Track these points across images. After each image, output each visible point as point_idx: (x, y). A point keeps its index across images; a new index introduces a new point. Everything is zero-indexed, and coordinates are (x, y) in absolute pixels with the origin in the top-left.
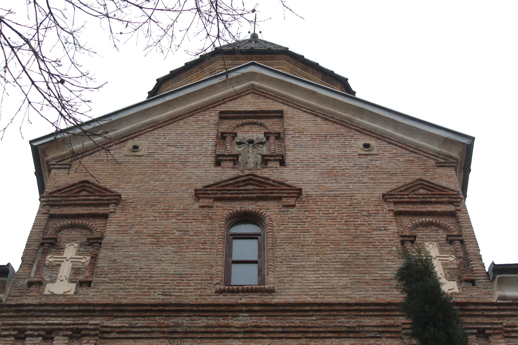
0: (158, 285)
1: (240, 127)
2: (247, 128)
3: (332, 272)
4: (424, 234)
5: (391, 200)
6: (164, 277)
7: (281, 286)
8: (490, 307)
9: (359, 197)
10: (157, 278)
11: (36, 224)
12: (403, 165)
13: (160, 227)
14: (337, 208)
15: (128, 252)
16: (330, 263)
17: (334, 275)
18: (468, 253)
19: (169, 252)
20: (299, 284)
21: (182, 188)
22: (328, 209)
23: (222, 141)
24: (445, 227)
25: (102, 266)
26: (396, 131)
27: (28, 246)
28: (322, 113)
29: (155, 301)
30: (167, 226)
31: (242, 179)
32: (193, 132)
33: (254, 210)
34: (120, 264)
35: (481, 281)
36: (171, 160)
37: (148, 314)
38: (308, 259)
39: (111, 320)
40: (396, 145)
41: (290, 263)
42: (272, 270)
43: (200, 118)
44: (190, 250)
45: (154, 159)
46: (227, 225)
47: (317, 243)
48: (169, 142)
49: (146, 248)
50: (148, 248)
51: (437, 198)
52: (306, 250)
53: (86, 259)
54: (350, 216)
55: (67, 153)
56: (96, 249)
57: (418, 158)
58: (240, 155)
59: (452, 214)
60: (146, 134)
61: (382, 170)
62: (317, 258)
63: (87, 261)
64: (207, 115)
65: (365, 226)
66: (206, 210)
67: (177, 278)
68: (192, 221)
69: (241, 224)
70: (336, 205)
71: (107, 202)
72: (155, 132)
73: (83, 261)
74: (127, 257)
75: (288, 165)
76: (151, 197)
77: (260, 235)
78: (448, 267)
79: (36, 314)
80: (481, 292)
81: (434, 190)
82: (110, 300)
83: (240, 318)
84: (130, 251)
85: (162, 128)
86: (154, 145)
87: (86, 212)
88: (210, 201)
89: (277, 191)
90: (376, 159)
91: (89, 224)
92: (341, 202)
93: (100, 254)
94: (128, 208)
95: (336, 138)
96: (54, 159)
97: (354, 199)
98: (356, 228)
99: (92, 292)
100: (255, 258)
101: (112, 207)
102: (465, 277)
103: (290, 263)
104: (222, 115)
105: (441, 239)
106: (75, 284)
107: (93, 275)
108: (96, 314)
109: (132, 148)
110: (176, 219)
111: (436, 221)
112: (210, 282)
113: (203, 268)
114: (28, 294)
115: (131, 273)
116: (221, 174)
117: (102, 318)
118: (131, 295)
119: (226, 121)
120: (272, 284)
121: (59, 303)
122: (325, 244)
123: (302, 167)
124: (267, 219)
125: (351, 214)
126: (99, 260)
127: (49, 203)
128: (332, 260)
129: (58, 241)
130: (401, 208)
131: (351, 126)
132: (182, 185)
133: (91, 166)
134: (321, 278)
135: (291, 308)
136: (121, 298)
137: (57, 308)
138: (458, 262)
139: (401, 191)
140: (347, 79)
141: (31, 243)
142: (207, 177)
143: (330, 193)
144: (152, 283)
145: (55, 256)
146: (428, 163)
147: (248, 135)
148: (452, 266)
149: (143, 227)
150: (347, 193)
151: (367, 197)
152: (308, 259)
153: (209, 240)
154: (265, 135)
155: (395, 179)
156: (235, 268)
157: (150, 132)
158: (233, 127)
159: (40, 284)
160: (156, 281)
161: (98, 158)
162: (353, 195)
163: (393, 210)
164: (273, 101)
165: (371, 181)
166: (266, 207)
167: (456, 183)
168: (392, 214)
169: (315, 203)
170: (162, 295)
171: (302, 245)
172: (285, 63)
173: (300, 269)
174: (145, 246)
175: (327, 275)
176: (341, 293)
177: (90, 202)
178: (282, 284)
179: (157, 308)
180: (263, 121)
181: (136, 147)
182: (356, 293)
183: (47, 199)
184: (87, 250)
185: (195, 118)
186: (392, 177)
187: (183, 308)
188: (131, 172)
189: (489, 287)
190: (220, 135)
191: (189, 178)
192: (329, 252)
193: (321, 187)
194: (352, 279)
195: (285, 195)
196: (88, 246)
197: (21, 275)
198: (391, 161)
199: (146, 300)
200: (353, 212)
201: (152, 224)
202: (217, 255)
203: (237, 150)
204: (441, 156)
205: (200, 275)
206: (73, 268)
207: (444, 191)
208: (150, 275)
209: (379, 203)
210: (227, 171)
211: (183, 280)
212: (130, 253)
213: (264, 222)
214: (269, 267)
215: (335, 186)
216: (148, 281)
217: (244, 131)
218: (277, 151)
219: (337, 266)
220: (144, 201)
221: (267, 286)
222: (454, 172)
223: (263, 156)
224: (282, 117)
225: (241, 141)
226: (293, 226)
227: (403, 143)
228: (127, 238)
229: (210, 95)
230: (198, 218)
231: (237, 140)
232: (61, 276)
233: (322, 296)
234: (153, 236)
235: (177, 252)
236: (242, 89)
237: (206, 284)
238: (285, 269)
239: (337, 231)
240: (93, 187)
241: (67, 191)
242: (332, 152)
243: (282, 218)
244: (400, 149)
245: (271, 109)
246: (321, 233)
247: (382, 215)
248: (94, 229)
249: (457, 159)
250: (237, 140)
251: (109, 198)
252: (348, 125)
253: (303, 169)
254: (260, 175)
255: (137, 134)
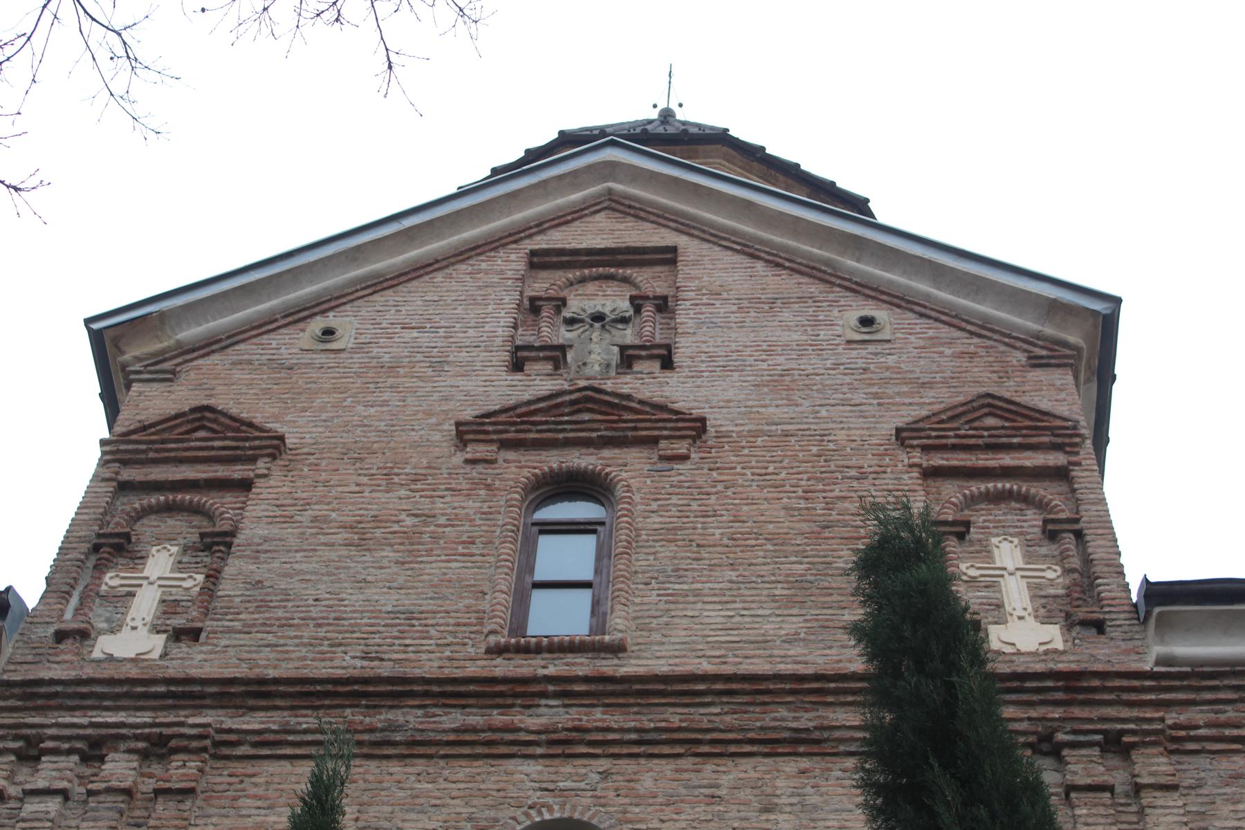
0: (355, 635)
1: (576, 286)
2: (591, 287)
3: (764, 605)
4: (991, 518)
5: (915, 442)
6: (369, 618)
7: (641, 636)
8: (1136, 683)
9: (841, 435)
10: (352, 621)
11: (86, 502)
12: (953, 364)
13: (370, 506)
14: (787, 461)
15: (291, 563)
16: (760, 586)
17: (768, 612)
18: (1092, 560)
19: (385, 563)
20: (684, 633)
21: (429, 421)
22: (766, 465)
23: (531, 317)
24: (1041, 501)
25: (229, 596)
26: (938, 289)
27: (65, 551)
28: (767, 250)
29: (344, 672)
30: (386, 506)
31: (567, 398)
32: (463, 298)
33: (591, 467)
34: (270, 590)
35: (1118, 623)
36: (408, 359)
37: (327, 702)
38: (711, 576)
39: (241, 716)
40: (936, 320)
41: (667, 585)
42: (623, 601)
43: (484, 266)
44: (434, 558)
45: (369, 357)
46: (527, 503)
47: (734, 539)
48: (407, 321)
49: (334, 555)
50: (339, 553)
51: (1024, 436)
52: (706, 555)
53: (195, 580)
54: (817, 478)
55: (169, 347)
56: (219, 557)
57: (986, 347)
58: (571, 346)
59: (1061, 474)
60: (356, 303)
61: (899, 376)
62: (731, 573)
63: (195, 586)
64: (500, 260)
65: (851, 502)
66: (480, 468)
67: (398, 621)
68: (446, 493)
69: (562, 501)
70: (784, 456)
71: (251, 452)
72: (376, 297)
73: (186, 584)
74: (286, 575)
75: (679, 367)
76: (356, 442)
77: (602, 524)
78: (1043, 593)
79: (69, 703)
80: (1118, 647)
81: (1019, 419)
82: (242, 671)
83: (543, 710)
84: (297, 562)
85: (394, 289)
86: (371, 327)
87: (204, 476)
88: (489, 448)
89: (648, 425)
90: (887, 351)
91: (206, 502)
92: (797, 448)
93: (226, 568)
94: (300, 466)
95: (797, 305)
96: (138, 359)
97: (829, 441)
98: (829, 506)
99: (201, 652)
100: (587, 574)
101: (261, 465)
102: (1081, 614)
103: (667, 585)
104: (535, 259)
105: (1030, 530)
106: (164, 636)
107: (206, 615)
108: (208, 702)
109: (320, 334)
110: (410, 490)
111: (1020, 488)
112: (475, 628)
113: (461, 598)
114: (52, 658)
115: (293, 609)
116: (523, 388)
117: (221, 712)
118: (291, 659)
119: (544, 274)
120: (621, 631)
121: (122, 676)
122: (753, 542)
123: (711, 371)
124: (619, 486)
125: (819, 475)
126: (223, 581)
127: (118, 456)
128: (766, 579)
129: (133, 540)
130: (938, 460)
131: (833, 279)
132: (429, 414)
133: (222, 375)
134: (738, 619)
135: (662, 687)
136: (266, 667)
137: (118, 690)
138: (1067, 582)
139: (942, 422)
140: (867, 201)
141: (70, 545)
142: (488, 396)
143: (774, 428)
144: (340, 632)
145: (122, 575)
146: (1009, 359)
147: (592, 303)
148: (1052, 591)
149: (330, 507)
150: (813, 427)
151: (861, 436)
152: (711, 576)
153: (481, 536)
154: (631, 303)
155: (929, 395)
156: (539, 599)
157: (366, 299)
158: (560, 287)
159: (84, 635)
160: (350, 629)
161: (241, 357)
162: (827, 432)
163: (919, 466)
164: (655, 226)
165: (872, 401)
166: (620, 461)
167: (1074, 404)
168: (916, 475)
169: (736, 451)
170: (363, 658)
171: (698, 546)
172: (720, 164)
173: (691, 599)
174: (330, 550)
175: (753, 612)
176: (782, 653)
177: (213, 453)
178: (644, 633)
179: (347, 689)
180: (629, 271)
181: (329, 332)
182: (819, 652)
183: (115, 449)
184: (199, 559)
185: (472, 265)
186: (922, 390)
187: (408, 688)
188: (314, 386)
189: (1137, 637)
190: (526, 302)
191: (446, 399)
192: (760, 560)
193: (752, 416)
194: (811, 620)
195: (665, 433)
196: (202, 551)
197: (41, 616)
198: (923, 355)
199: (323, 670)
200: (823, 469)
201: (352, 500)
202: (498, 567)
203: (564, 335)
204: (1040, 343)
205: (452, 614)
206: (164, 601)
207: (1043, 421)
208: (338, 614)
209: (886, 450)
210: (536, 382)
211: (414, 626)
212: (296, 566)
213: (613, 495)
214: (617, 593)
215: (785, 412)
216: (330, 628)
217: (586, 295)
218: (658, 336)
219: (777, 592)
220: (338, 450)
221: (607, 638)
222: (1070, 378)
223: (623, 348)
224: (673, 262)
225: (575, 316)
226: (680, 502)
227: (954, 313)
228: (290, 533)
229: (510, 214)
230: (459, 487)
231: (567, 313)
232: (133, 619)
233: (736, 660)
234: (351, 527)
235: (403, 563)
236: (584, 200)
237: (467, 635)
238: (654, 598)
239: (782, 513)
240: (222, 419)
241: (164, 430)
242: (785, 337)
243: (657, 485)
244: (946, 329)
245: (649, 245)
246: (745, 519)
247: (891, 476)
248: (217, 513)
249: (1078, 349)
250: (567, 313)
251: (257, 443)
252: (827, 277)
253: (712, 376)
254: (609, 390)
255: (333, 303)
